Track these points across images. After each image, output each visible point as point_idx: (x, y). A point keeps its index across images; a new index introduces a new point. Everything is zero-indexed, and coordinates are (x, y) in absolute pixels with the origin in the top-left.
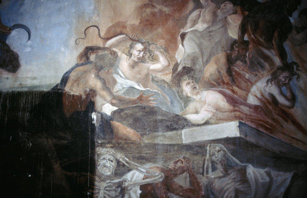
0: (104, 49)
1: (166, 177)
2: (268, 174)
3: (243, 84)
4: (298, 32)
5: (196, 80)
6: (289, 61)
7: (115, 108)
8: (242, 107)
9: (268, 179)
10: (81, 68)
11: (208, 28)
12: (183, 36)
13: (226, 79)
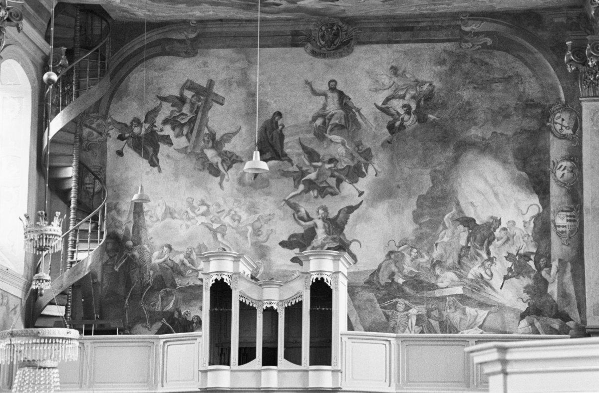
0: (398, 252)
1: (428, 312)
2: (476, 311)
3: (466, 268)
4: (498, 241)
5: (442, 267)
6: (492, 256)
7: (404, 281)
8: (465, 280)
9: (476, 313)
10: (387, 262)
11: (450, 240)
12: (437, 245)
13: (458, 266)
